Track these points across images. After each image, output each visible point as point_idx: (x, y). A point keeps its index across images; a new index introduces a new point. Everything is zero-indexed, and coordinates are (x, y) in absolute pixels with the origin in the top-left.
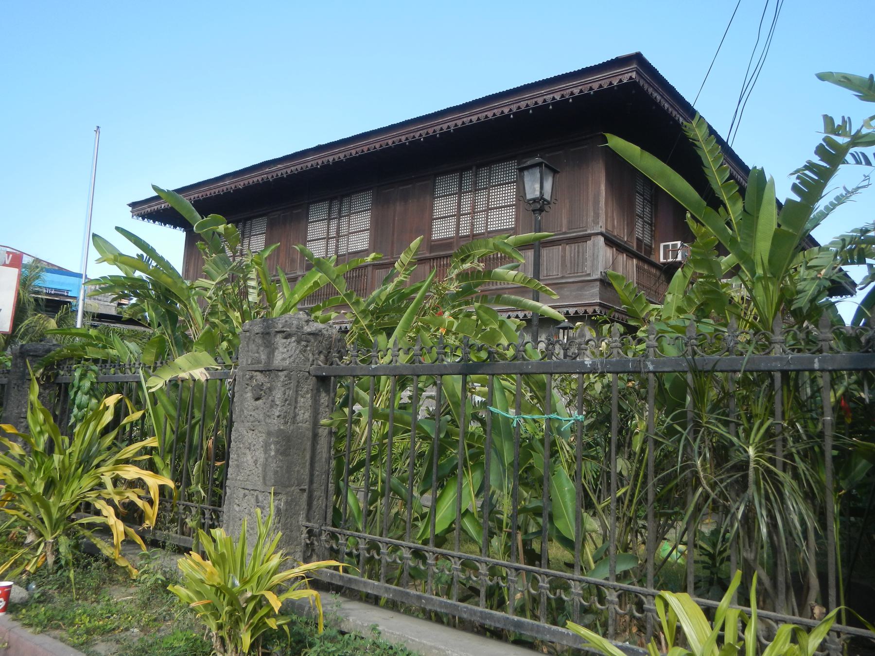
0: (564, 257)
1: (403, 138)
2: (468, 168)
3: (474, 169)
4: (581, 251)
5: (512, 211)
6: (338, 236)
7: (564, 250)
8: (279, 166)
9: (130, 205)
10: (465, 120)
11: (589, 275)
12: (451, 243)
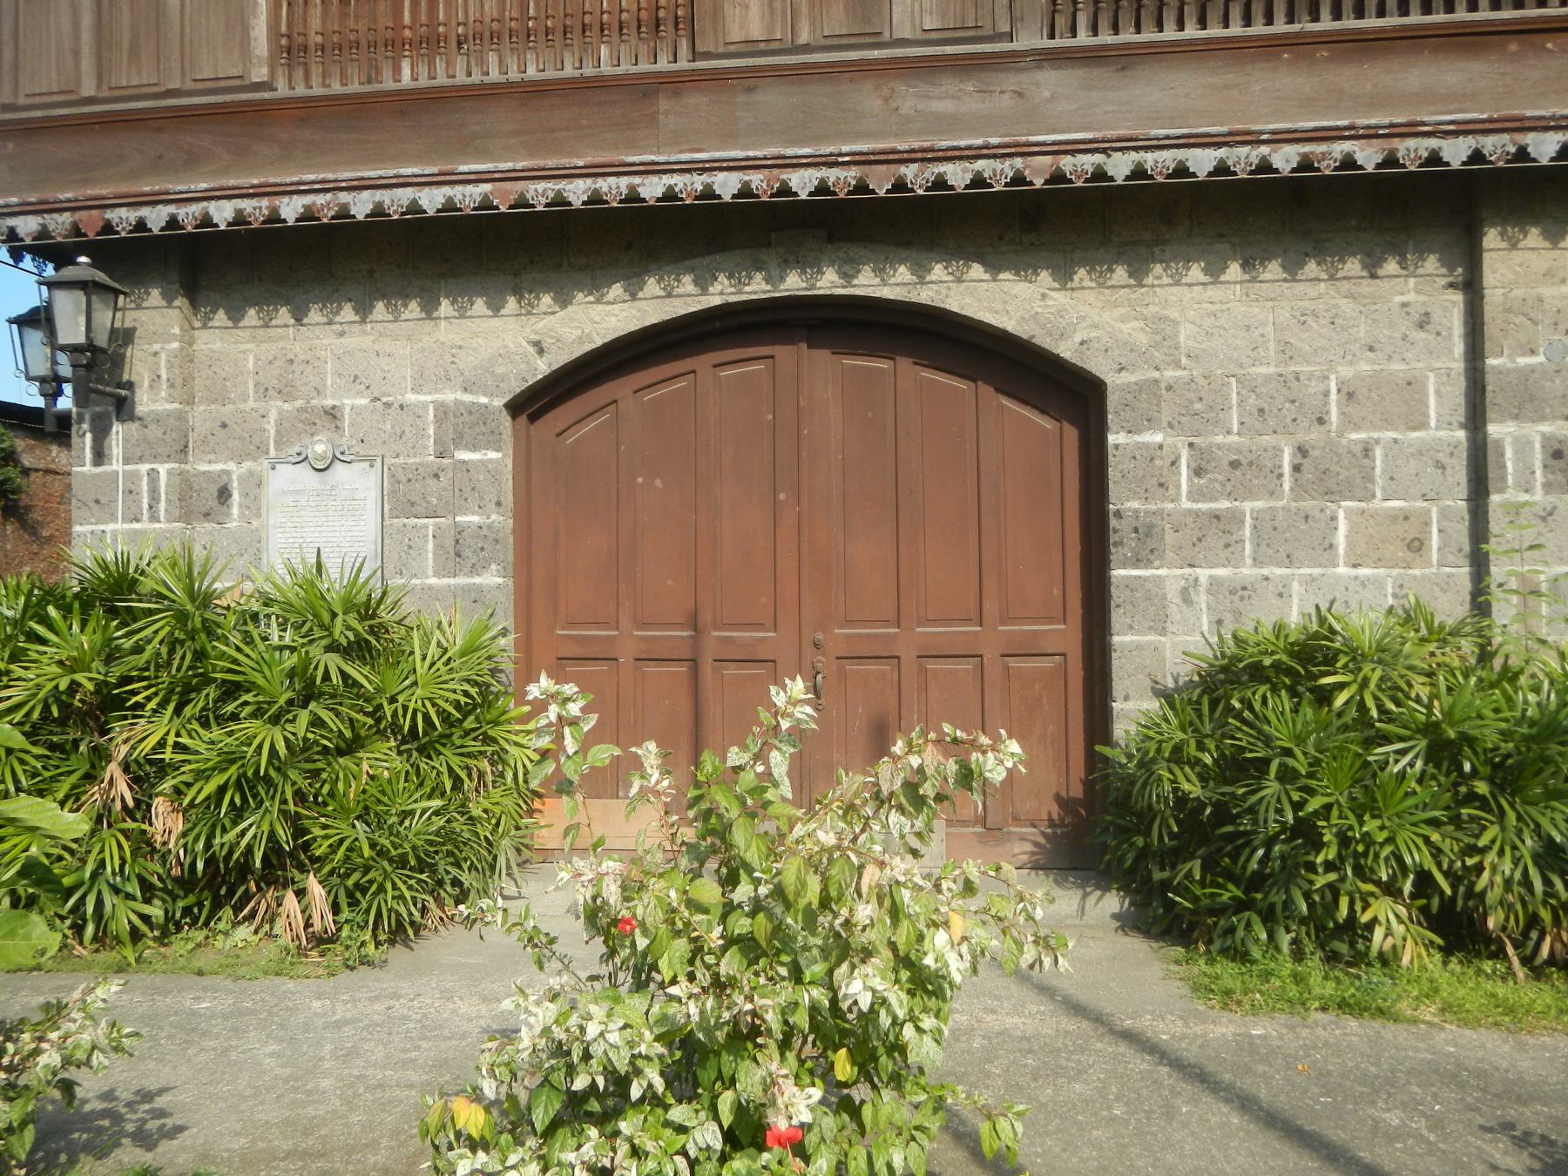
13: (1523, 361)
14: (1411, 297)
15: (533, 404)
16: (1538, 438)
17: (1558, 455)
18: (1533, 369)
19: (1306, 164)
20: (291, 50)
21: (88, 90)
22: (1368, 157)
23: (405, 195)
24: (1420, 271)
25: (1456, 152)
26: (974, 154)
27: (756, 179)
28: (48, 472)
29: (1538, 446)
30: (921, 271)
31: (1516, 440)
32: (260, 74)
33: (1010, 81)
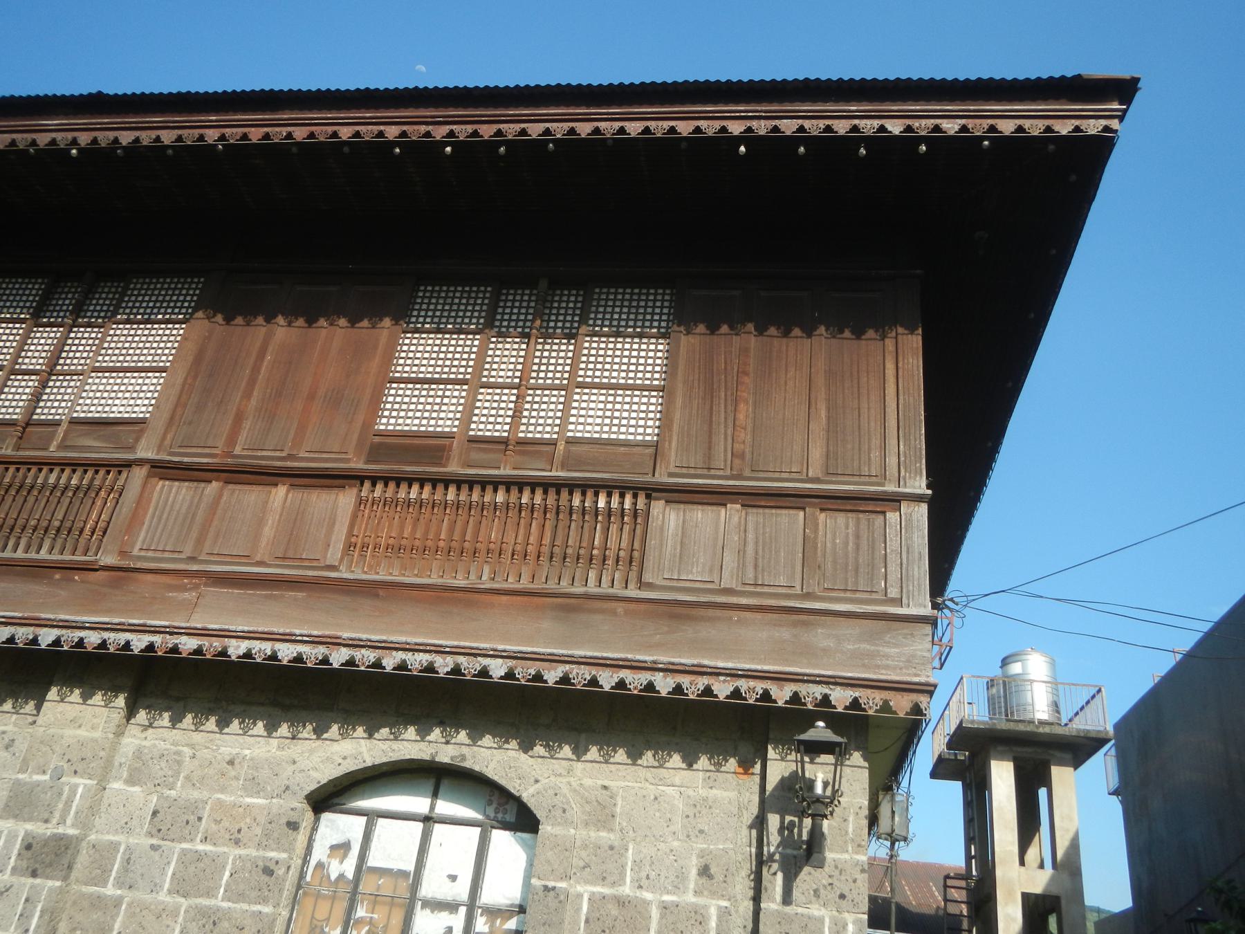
0: (808, 544)
2: (528, 282)
3: (543, 284)
4: (864, 534)
5: (654, 402)
6: (51, 371)
10: (602, 125)
11: (899, 602)
12: (442, 449)
13: (37, 777)
14: (9, 728)
16: (22, 834)
17: (28, 847)
18: (38, 784)
24: (22, 711)
29: (20, 839)
31: (9, 832)
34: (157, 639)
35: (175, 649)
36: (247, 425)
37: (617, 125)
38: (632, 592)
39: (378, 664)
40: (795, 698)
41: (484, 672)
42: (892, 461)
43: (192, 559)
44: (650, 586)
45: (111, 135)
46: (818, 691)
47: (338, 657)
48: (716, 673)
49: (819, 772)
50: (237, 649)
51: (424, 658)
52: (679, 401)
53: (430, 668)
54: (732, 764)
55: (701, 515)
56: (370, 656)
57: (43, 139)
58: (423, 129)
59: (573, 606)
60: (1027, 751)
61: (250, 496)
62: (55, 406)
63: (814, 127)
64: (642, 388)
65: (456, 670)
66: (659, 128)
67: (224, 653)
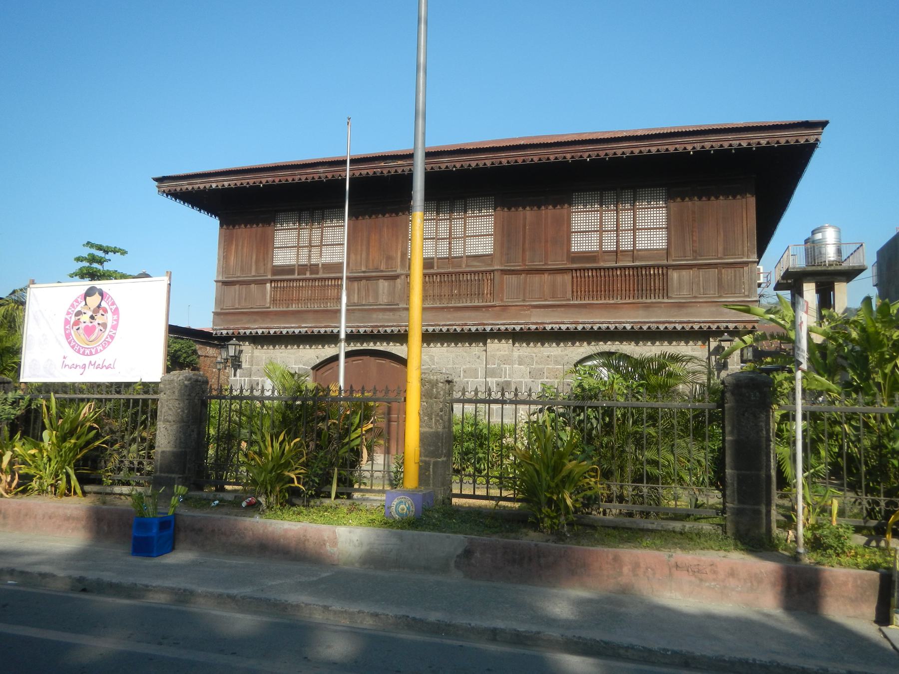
0: (720, 280)
1: (568, 156)
4: (738, 275)
5: (663, 234)
7: (720, 273)
8: (400, 162)
9: (156, 180)
11: (748, 296)
12: (595, 256)
15: (317, 368)
19: (448, 330)
20: (274, 301)
21: (237, 306)
22: (459, 329)
23: (292, 330)
25: (473, 329)
26: (392, 326)
27: (354, 329)
28: (206, 356)
30: (388, 344)
32: (268, 305)
33: (398, 313)
34: (523, 326)
35: (529, 329)
36: (527, 253)
37: (648, 149)
38: (666, 300)
39: (592, 328)
40: (718, 328)
41: (624, 328)
42: (746, 249)
43: (524, 300)
44: (671, 298)
45: (468, 163)
46: (725, 325)
47: (580, 327)
48: (694, 322)
49: (726, 345)
50: (548, 327)
51: (606, 325)
52: (673, 233)
53: (608, 328)
54: (700, 343)
55: (684, 273)
56: (590, 326)
57: (443, 166)
58: (579, 154)
59: (647, 306)
60: (823, 279)
61: (536, 278)
62: (458, 251)
63: (716, 145)
64: (660, 228)
65: (616, 328)
66: (663, 149)
67: (545, 328)
